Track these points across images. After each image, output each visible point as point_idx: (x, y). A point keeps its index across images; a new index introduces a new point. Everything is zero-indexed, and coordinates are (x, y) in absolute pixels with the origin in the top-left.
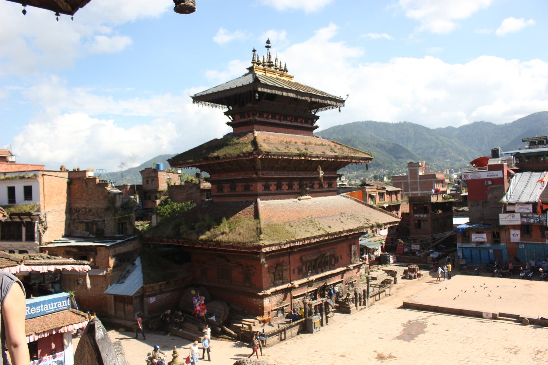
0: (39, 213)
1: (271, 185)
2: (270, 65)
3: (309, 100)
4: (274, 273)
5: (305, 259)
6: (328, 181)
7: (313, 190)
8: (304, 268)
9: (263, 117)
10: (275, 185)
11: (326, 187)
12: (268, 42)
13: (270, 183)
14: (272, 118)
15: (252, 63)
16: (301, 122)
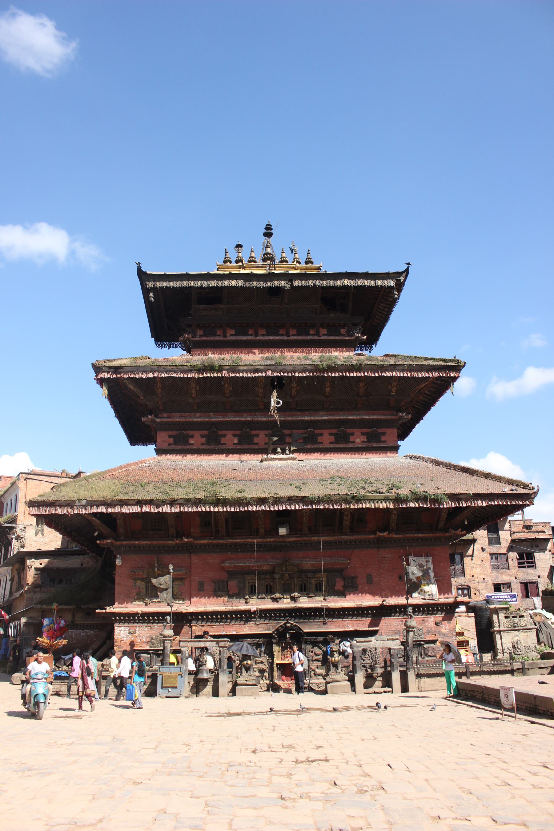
0: (14, 525)
1: (192, 436)
2: (268, 257)
3: (288, 286)
4: (146, 582)
5: (227, 564)
6: (365, 430)
7: (315, 446)
8: (233, 584)
9: (215, 335)
10: (202, 436)
11: (358, 440)
12: (268, 228)
13: (191, 433)
14: (236, 334)
15: (225, 262)
16: (318, 334)
